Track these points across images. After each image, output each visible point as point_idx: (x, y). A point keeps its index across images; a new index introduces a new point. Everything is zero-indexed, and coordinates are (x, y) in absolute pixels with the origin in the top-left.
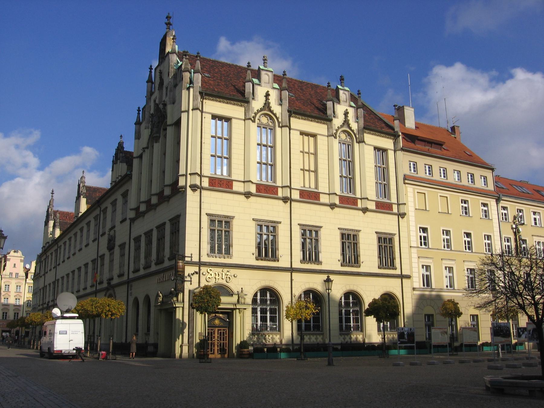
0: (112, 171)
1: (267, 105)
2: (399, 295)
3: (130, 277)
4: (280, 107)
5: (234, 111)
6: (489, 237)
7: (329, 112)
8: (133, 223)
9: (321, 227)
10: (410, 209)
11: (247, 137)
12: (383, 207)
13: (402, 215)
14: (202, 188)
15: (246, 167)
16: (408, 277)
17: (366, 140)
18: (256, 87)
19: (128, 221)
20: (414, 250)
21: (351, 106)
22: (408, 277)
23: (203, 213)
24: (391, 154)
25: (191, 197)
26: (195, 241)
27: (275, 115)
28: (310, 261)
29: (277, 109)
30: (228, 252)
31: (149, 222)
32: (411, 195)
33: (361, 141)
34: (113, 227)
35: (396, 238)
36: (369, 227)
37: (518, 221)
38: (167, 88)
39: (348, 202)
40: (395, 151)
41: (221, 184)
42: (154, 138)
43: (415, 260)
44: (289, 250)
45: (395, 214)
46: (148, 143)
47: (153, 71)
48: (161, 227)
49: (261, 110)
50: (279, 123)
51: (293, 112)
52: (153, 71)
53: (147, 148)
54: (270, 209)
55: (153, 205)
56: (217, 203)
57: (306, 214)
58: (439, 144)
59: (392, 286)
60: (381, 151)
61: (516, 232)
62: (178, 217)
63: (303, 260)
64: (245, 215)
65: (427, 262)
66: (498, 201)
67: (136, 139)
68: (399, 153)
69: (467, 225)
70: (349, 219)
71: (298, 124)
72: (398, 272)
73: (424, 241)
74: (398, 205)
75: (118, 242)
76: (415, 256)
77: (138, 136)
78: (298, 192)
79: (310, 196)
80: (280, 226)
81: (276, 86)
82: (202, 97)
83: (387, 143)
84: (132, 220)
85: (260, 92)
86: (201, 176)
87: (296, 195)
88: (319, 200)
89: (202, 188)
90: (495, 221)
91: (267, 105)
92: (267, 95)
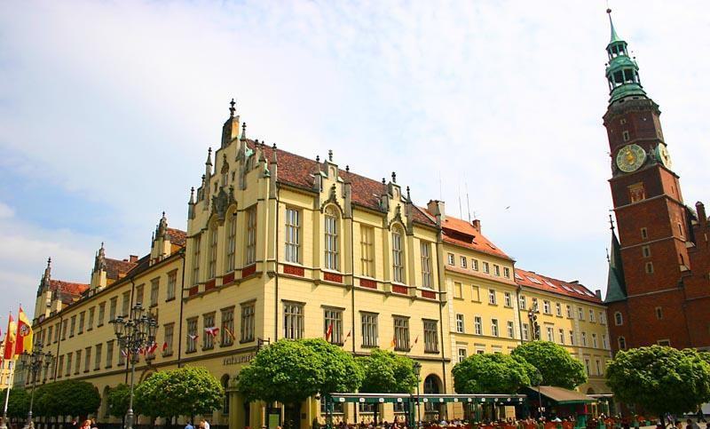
0: (153, 246)
1: (333, 198)
2: (442, 379)
3: (181, 357)
4: (343, 200)
5: (305, 203)
6: (510, 324)
7: (385, 206)
8: (186, 303)
9: (409, 318)
10: (449, 298)
11: (314, 226)
12: (428, 295)
13: (442, 304)
14: (278, 276)
15: (313, 256)
16: (449, 361)
17: (415, 234)
18: (324, 180)
19: (178, 300)
20: (452, 336)
21: (402, 201)
22: (449, 361)
23: (279, 300)
24: (433, 246)
25: (269, 285)
27: (339, 206)
28: (369, 347)
29: (341, 201)
33: (410, 234)
34: (154, 305)
35: (438, 324)
38: (234, 174)
39: (401, 290)
40: (437, 244)
41: (295, 272)
43: (454, 344)
45: (437, 302)
46: (207, 225)
47: (213, 154)
48: (228, 311)
49: (328, 201)
50: (343, 215)
51: (355, 206)
52: (213, 154)
53: (206, 229)
54: (334, 296)
55: (217, 287)
56: (291, 289)
57: (367, 301)
58: (469, 238)
59: (436, 369)
60: (425, 244)
62: (255, 300)
63: (363, 346)
65: (463, 347)
67: (189, 218)
68: (440, 246)
69: (477, 310)
70: (400, 306)
71: (360, 218)
72: (440, 356)
74: (440, 294)
75: (161, 322)
76: (454, 341)
77: (192, 215)
78: (359, 281)
79: (369, 285)
80: (344, 312)
81: (340, 179)
82: (279, 188)
83: (430, 237)
84: (184, 300)
85: (327, 184)
86: (278, 264)
87: (357, 283)
88: (376, 288)
89: (278, 276)
90: (516, 309)
91: (333, 198)
92: (334, 188)
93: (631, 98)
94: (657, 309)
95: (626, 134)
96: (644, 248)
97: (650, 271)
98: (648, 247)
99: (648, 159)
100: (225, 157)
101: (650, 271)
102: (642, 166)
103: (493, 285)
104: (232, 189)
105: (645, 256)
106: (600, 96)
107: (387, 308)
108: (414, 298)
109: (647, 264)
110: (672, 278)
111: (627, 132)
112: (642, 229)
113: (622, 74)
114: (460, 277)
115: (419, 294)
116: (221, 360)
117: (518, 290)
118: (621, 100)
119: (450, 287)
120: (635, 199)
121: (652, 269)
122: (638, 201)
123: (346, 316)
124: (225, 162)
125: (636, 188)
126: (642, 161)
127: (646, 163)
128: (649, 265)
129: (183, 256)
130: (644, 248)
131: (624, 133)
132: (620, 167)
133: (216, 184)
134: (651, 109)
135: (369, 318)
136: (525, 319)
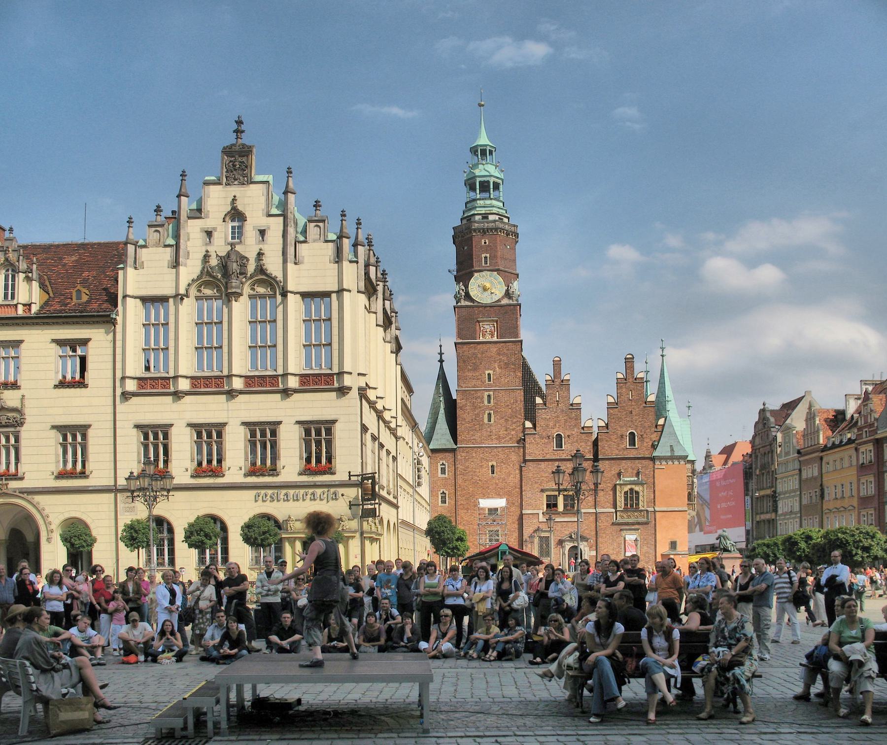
38: (262, 233)
53: (187, 296)
93: (497, 217)
94: (490, 464)
95: (486, 258)
96: (487, 393)
97: (490, 420)
98: (491, 393)
99: (508, 294)
100: (234, 199)
101: (490, 420)
102: (499, 301)
104: (260, 255)
105: (486, 402)
109: (487, 412)
110: (513, 433)
111: (488, 255)
112: (487, 372)
116: (253, 493)
118: (485, 216)
120: (484, 336)
121: (492, 419)
122: (488, 338)
124: (234, 208)
127: (503, 298)
128: (489, 414)
129: (114, 322)
130: (487, 393)
131: (483, 255)
132: (472, 294)
133: (209, 234)
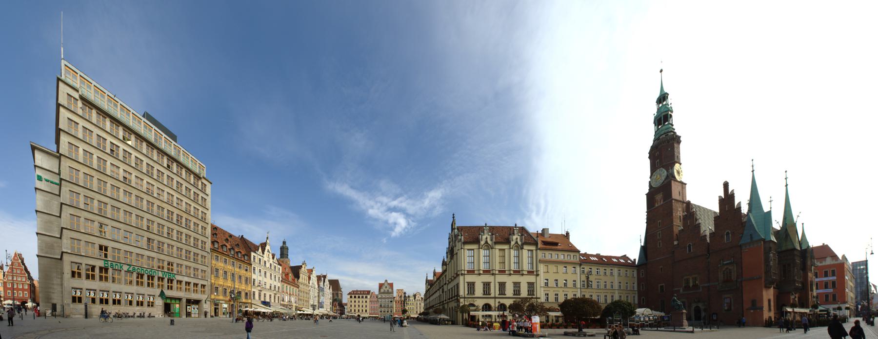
10: (541, 272)
12: (530, 273)
13: (537, 275)
25: (461, 278)
26: (463, 291)
30: (474, 294)
31: (450, 286)
32: (542, 268)
36: (524, 281)
37: (590, 273)
39: (517, 272)
41: (471, 272)
42: (452, 258)
44: (494, 290)
56: (470, 278)
57: (501, 278)
61: (588, 278)
64: (479, 282)
66: (580, 265)
70: (516, 278)
73: (547, 284)
103: (565, 263)
106: (647, 136)
107: (509, 281)
108: (523, 275)
113: (663, 118)
114: (546, 262)
115: (525, 273)
117: (580, 265)
119: (542, 268)
123: (492, 285)
125: (659, 197)
126: (663, 178)
134: (677, 140)
135: (502, 285)
136: (584, 278)
